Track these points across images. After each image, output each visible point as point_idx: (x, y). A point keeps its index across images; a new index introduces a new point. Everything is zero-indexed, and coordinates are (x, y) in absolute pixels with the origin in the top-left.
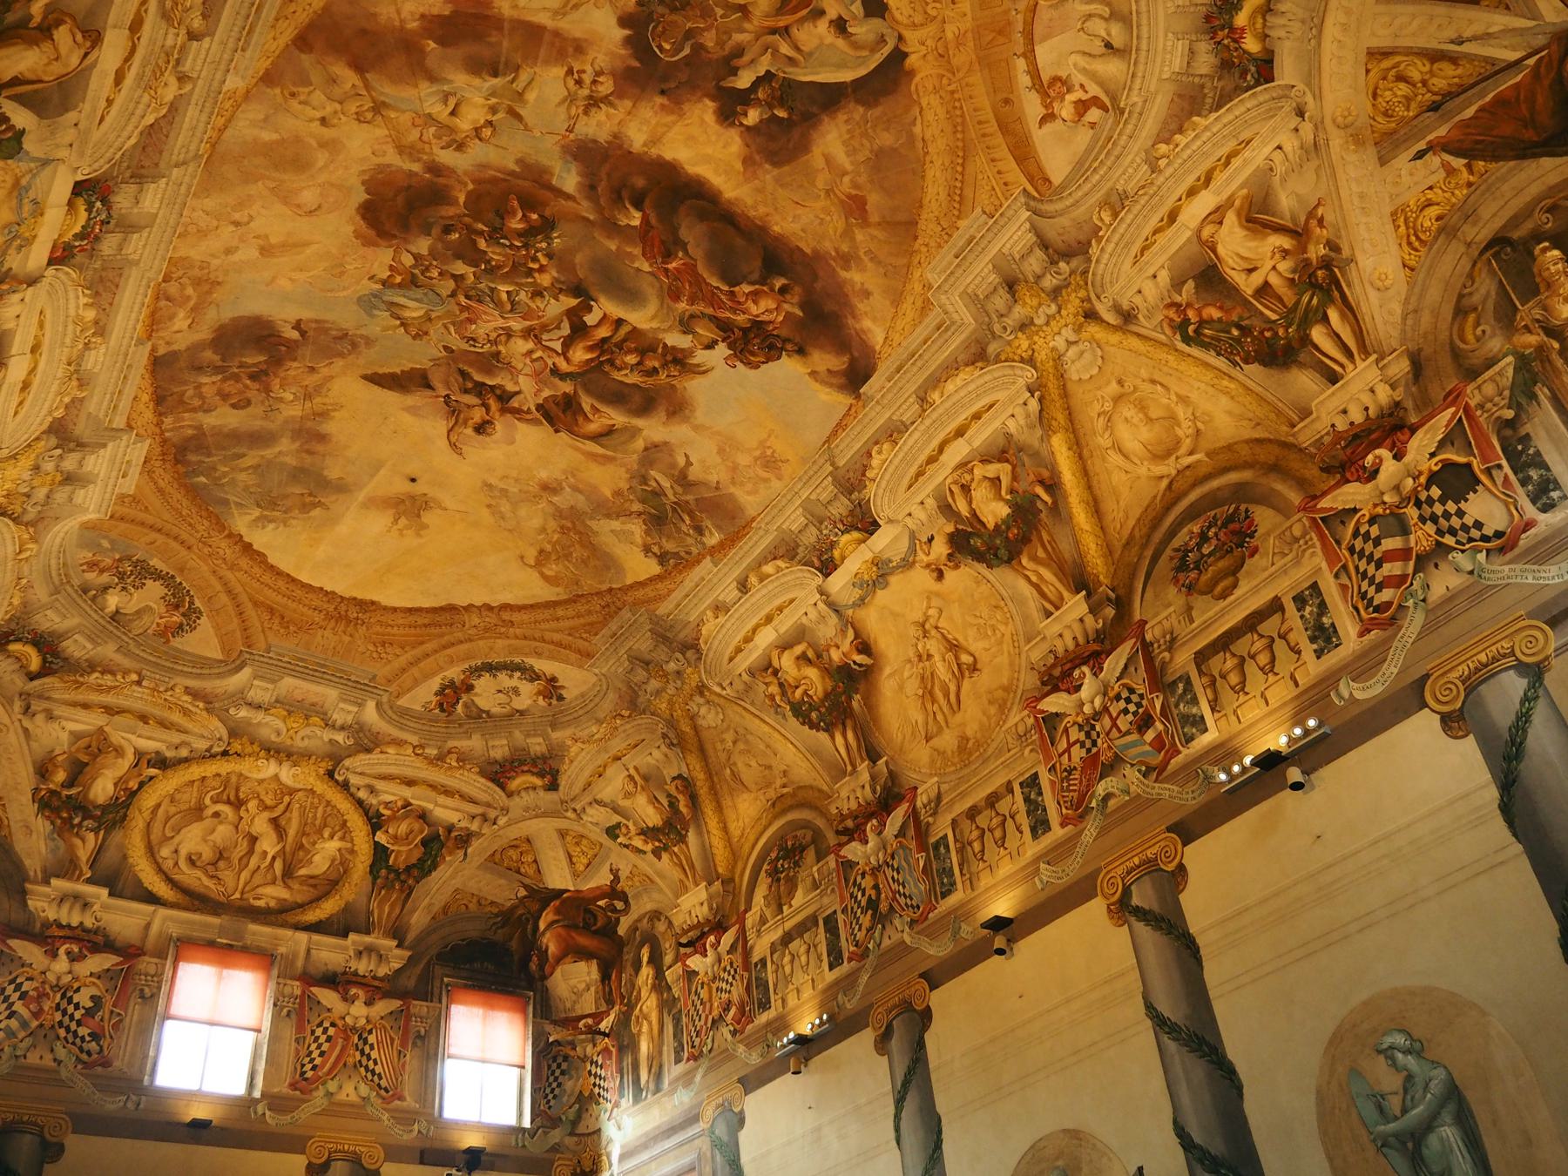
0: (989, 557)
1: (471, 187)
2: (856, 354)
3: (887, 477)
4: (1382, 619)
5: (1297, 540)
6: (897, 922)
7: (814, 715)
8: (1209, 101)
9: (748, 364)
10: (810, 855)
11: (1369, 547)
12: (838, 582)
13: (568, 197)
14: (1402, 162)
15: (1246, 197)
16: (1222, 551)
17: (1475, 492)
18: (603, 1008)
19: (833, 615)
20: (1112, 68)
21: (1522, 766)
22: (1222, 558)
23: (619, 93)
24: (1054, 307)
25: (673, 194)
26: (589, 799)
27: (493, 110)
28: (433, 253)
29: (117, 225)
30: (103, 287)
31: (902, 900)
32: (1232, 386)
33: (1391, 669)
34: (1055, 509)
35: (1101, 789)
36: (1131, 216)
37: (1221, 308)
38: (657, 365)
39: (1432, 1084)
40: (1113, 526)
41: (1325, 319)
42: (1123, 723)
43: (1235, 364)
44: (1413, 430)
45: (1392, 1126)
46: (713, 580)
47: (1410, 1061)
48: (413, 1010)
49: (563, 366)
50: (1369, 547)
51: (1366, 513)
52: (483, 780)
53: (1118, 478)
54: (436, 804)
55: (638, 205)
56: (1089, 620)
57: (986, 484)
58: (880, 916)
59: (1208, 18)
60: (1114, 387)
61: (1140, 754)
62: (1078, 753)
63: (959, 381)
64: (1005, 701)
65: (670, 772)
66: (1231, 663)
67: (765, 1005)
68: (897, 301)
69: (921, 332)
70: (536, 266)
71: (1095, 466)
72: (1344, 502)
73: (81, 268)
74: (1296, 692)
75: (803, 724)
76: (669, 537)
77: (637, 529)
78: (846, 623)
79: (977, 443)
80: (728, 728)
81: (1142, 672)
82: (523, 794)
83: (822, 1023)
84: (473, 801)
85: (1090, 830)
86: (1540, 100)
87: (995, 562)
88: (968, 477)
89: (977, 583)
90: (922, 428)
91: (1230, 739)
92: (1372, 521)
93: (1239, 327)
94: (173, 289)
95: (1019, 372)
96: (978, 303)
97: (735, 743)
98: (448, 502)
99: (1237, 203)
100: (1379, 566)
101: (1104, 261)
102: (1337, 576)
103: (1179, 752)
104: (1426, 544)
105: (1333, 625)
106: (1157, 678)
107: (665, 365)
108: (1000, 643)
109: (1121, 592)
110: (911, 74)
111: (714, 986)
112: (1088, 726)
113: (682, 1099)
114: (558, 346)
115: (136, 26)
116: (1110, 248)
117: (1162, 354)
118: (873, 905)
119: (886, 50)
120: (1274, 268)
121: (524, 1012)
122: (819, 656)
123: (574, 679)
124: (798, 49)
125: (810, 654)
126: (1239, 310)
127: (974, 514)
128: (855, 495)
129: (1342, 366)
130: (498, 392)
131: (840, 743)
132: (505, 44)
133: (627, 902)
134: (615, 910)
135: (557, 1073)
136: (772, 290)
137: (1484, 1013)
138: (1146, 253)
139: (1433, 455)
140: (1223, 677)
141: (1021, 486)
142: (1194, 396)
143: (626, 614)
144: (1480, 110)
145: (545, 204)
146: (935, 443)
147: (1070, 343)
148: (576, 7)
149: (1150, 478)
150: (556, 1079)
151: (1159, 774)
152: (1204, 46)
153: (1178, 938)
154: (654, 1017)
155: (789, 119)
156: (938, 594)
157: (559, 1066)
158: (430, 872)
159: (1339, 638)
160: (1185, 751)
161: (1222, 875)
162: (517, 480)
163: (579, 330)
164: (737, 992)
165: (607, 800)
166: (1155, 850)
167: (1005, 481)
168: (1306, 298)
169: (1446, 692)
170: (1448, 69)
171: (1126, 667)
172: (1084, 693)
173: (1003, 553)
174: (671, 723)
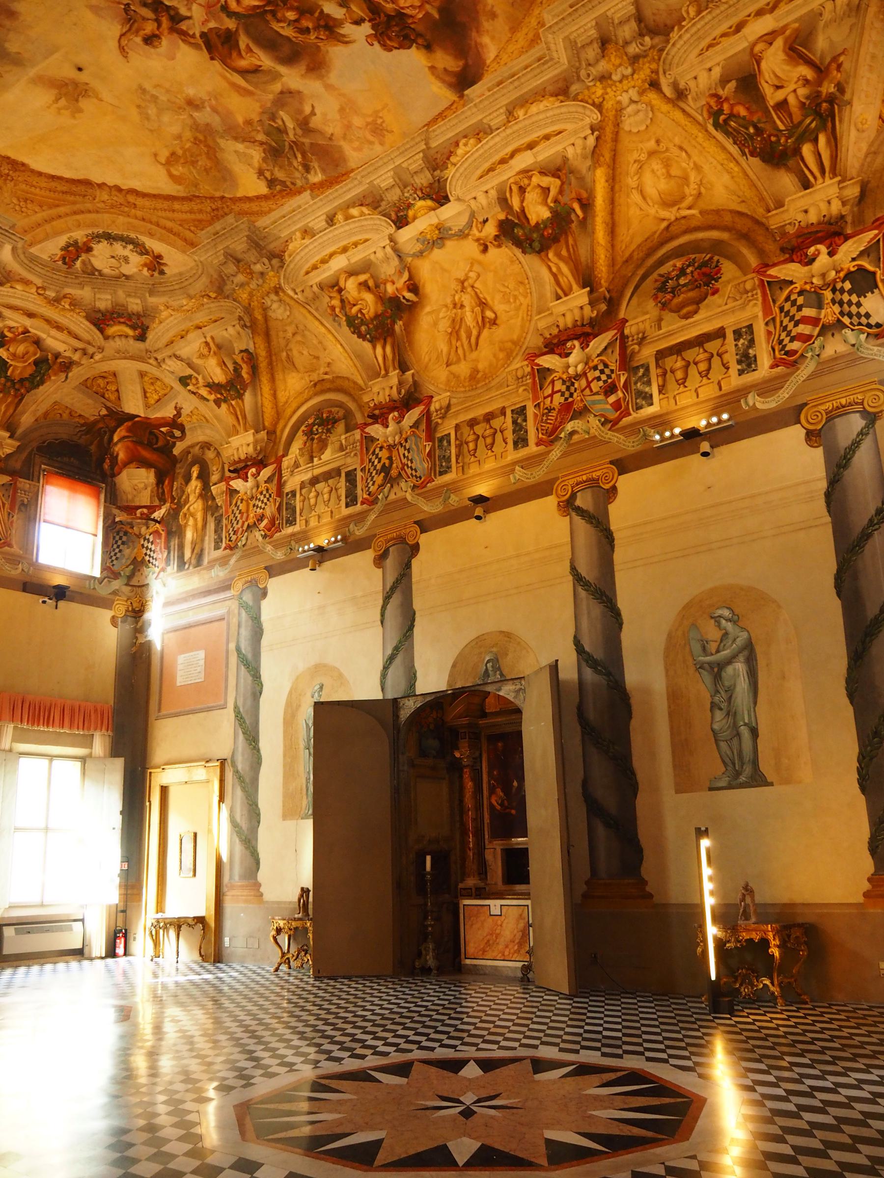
2: (470, 62)
3: (465, 165)
4: (789, 361)
5: (747, 292)
6: (403, 484)
7: (363, 328)
10: (341, 427)
11: (793, 310)
12: (406, 235)
16: (694, 285)
17: (873, 293)
18: (157, 503)
19: (396, 259)
21: (845, 473)
22: (690, 290)
26: (168, 352)
31: (409, 471)
32: (736, 169)
33: (784, 395)
35: (570, 426)
36: (709, 17)
37: (748, 109)
38: (311, 26)
39: (738, 640)
40: (620, 246)
41: (816, 141)
42: (595, 386)
43: (744, 154)
44: (847, 238)
45: (708, 659)
46: (308, 209)
47: (729, 626)
48: (19, 485)
50: (793, 310)
51: (798, 286)
52: (88, 323)
53: (634, 212)
54: (49, 336)
56: (587, 309)
57: (538, 190)
58: (389, 477)
60: (651, 144)
61: (602, 410)
62: (558, 399)
63: (542, 106)
64: (512, 351)
65: (239, 346)
66: (680, 364)
67: (291, 522)
68: (514, 30)
69: (526, 59)
71: (621, 199)
72: (786, 275)
74: (719, 393)
75: (353, 333)
76: (281, 167)
77: (256, 155)
78: (405, 267)
79: (540, 158)
80: (291, 323)
81: (617, 355)
82: (117, 339)
83: (336, 541)
84: (76, 337)
85: (556, 452)
87: (529, 250)
88: (526, 181)
89: (512, 262)
90: (503, 135)
91: (667, 414)
92: (800, 293)
93: (756, 127)
95: (588, 112)
96: (575, 49)
97: (294, 334)
98: (105, 95)
99: (788, 32)
100: (796, 325)
101: (678, 46)
102: (767, 324)
103: (630, 414)
104: (831, 319)
105: (755, 356)
106: (626, 361)
107: (317, 28)
108: (517, 309)
109: (614, 295)
111: (252, 503)
112: (569, 382)
113: (219, 573)
117: (694, 130)
118: (386, 470)
120: (795, 91)
121: (98, 499)
122: (377, 286)
123: (176, 260)
125: (371, 283)
126: (760, 114)
127: (523, 210)
128: (437, 173)
129: (815, 178)
130: (172, 13)
131: (380, 353)
133: (183, 430)
134: (173, 436)
135: (119, 543)
137: (779, 607)
138: (711, 50)
139: (854, 259)
140: (673, 371)
141: (563, 199)
142: (706, 168)
143: (230, 219)
146: (509, 149)
147: (632, 101)
149: (656, 218)
150: (118, 547)
151: (613, 426)
153: (602, 531)
154: (199, 516)
156: (480, 263)
157: (121, 538)
158: (38, 386)
159: (756, 366)
160: (634, 415)
161: (638, 499)
162: (168, 91)
164: (270, 510)
165: (184, 356)
166: (598, 473)
167: (553, 192)
168: (808, 121)
169: (813, 418)
171: (606, 348)
172: (572, 359)
173: (536, 245)
174: (248, 310)
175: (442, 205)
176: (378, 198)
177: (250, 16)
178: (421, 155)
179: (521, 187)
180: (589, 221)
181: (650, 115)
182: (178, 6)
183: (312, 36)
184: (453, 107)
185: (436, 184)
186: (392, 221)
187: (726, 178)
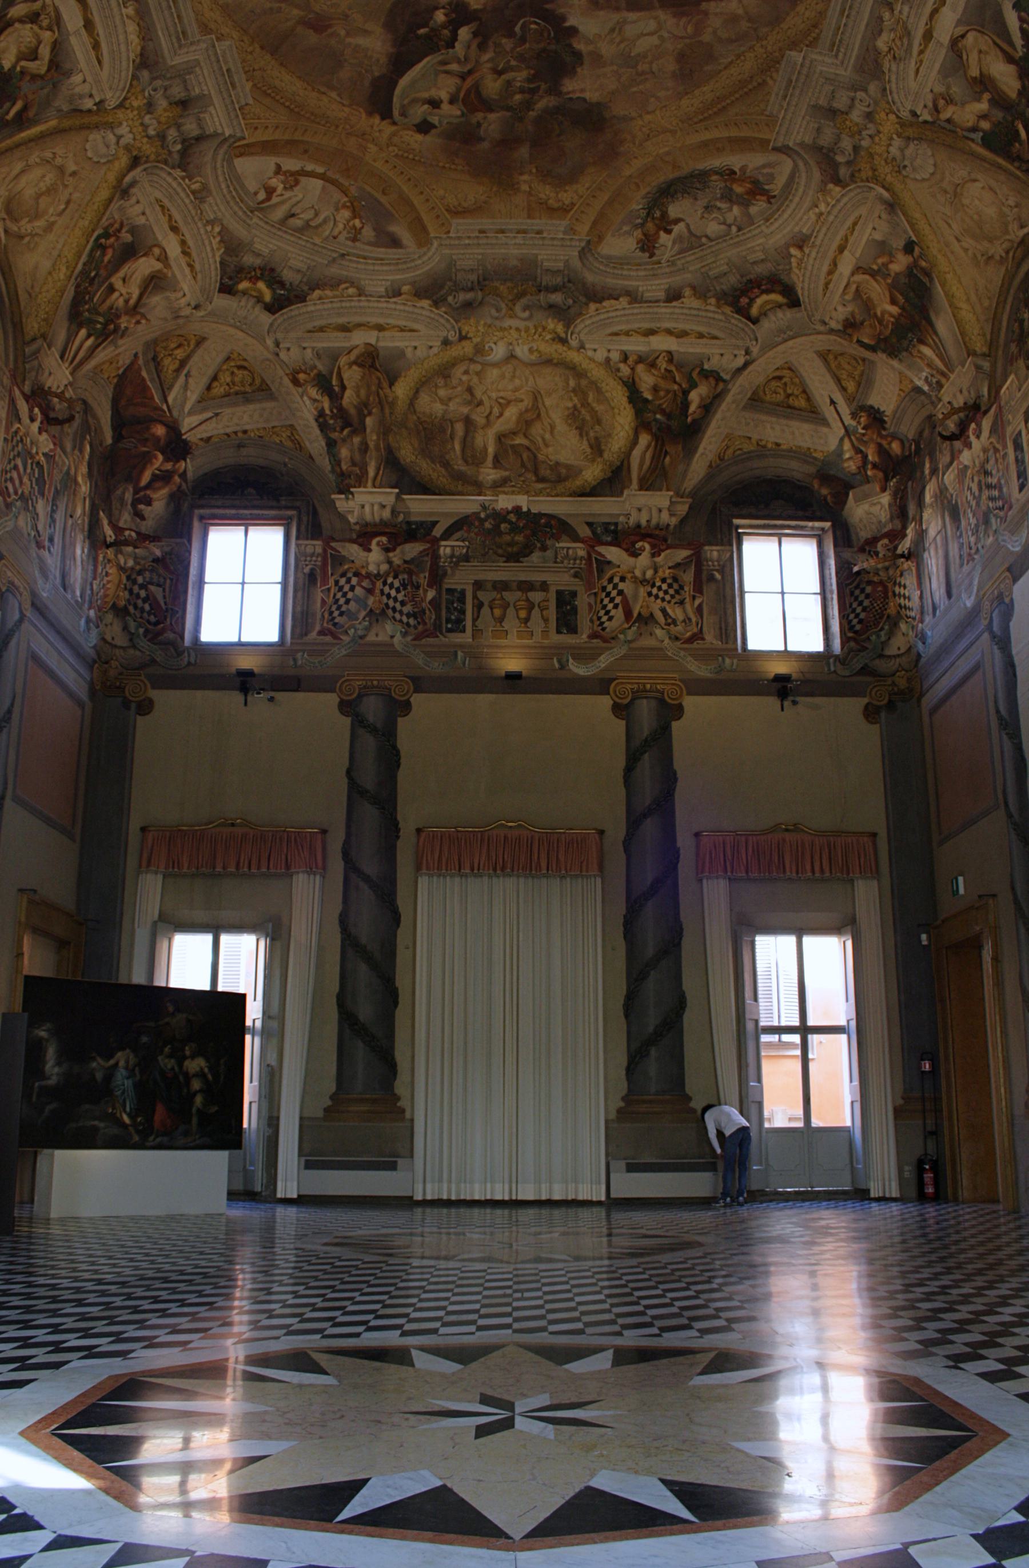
8: (227, 258)
14: (140, 349)
15: (165, 276)
20: (279, 213)
24: (151, 132)
32: (62, 277)
37: (109, 262)
59: (272, 270)
60: (72, 167)
63: (134, 39)
79: (73, 40)
95: (118, 94)
96: (183, 74)
110: (370, 114)
116: (174, 185)
119: (396, 113)
124: (447, 72)
141: (26, 86)
142: (51, 237)
144: (143, 379)
147: (119, 138)
148: (613, 30)
152: (258, 262)
168: (101, 319)
170: (172, 367)
181: (103, 161)
187: (46, 265)
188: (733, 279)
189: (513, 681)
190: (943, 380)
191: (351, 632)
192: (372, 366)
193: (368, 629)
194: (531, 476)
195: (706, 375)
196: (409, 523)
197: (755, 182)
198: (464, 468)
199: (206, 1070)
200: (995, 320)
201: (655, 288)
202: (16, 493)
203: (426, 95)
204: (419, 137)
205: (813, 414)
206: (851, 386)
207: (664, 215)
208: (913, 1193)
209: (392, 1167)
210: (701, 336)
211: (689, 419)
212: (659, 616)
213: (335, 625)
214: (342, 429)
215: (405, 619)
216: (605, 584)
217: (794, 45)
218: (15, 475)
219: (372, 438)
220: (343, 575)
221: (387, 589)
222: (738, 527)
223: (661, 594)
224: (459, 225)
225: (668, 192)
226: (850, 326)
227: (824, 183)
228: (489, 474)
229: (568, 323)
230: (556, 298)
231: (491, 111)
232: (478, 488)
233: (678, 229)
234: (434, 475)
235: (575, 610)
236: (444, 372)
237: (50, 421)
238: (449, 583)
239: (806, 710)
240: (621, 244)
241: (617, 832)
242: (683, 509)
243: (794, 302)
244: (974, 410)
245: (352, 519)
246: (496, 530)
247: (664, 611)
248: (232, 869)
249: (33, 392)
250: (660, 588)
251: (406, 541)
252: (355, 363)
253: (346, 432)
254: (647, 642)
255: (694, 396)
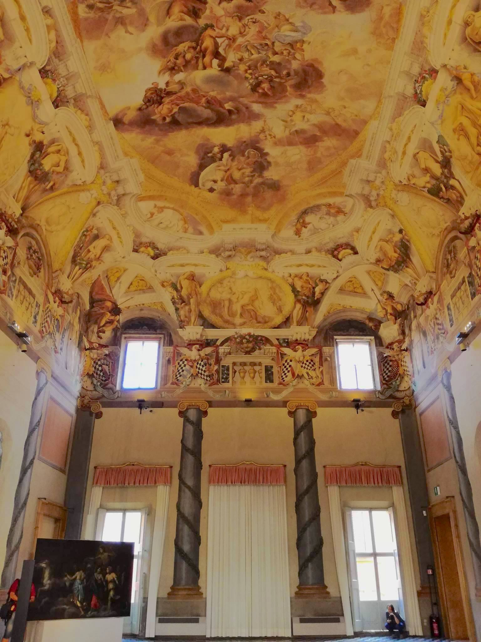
0: (33, 160)
1: (287, 94)
2: (126, 126)
9: (150, 89)
13: (253, 102)
20: (156, 222)
23: (257, 136)
25: (221, 120)
27: (292, 121)
28: (289, 62)
29: (412, 78)
30: (419, 47)
34: (45, 190)
41: (80, 269)
49: (209, 32)
55: (230, 111)
57: (58, 160)
59: (154, 243)
70: (249, 71)
73: (427, 61)
86: (102, 296)
87: (30, 164)
94: (391, 34)
107: (175, 64)
110: (190, 185)
114: (219, 40)
115: (404, 153)
127: (48, 154)
128: (72, 101)
132: (297, 139)
136: (168, 116)
141: (55, 177)
145: (260, 97)
148: (283, 153)
152: (147, 240)
155: (207, 156)
163: (216, 55)
175: (53, 103)
176: (61, 58)
177: (200, 36)
178: (84, 92)
179: (60, 150)
180: (46, 193)
182: (230, 4)
183: (172, 59)
184: (106, 114)
185: (66, 100)
186: (45, 66)
188: (331, 245)
189: (248, 403)
190: (417, 282)
191: (184, 383)
192: (193, 280)
193: (191, 382)
194: (254, 321)
195: (322, 281)
196: (207, 340)
197: (339, 208)
198: (228, 318)
199: (116, 579)
200: (437, 258)
201: (301, 249)
202: (46, 332)
203: (212, 178)
204: (210, 194)
205: (364, 294)
206: (380, 283)
207: (304, 221)
208: (429, 633)
209: (197, 621)
210: (319, 266)
211: (316, 299)
212: (306, 375)
213: (178, 380)
214: (181, 304)
215: (205, 378)
216: (284, 362)
217: (352, 157)
218: (46, 324)
219: (193, 307)
220: (181, 360)
221: (198, 366)
222: (336, 339)
223: (306, 367)
224: (226, 227)
225: (305, 213)
226: (378, 261)
227: (366, 208)
228: (238, 320)
229: (268, 263)
230: (263, 253)
231: (236, 183)
232: (234, 325)
233: (309, 227)
234: (217, 321)
235: (272, 373)
236: (221, 282)
237: (62, 302)
238: (223, 363)
239: (367, 413)
240: (288, 232)
241: (291, 465)
242: (314, 333)
243: (356, 253)
244: (430, 294)
245: (185, 338)
246: (241, 343)
247: (308, 373)
248: (132, 484)
249: (56, 292)
250: (306, 364)
251: (206, 347)
252: (186, 278)
253: (183, 304)
254: (301, 386)
255: (318, 290)
